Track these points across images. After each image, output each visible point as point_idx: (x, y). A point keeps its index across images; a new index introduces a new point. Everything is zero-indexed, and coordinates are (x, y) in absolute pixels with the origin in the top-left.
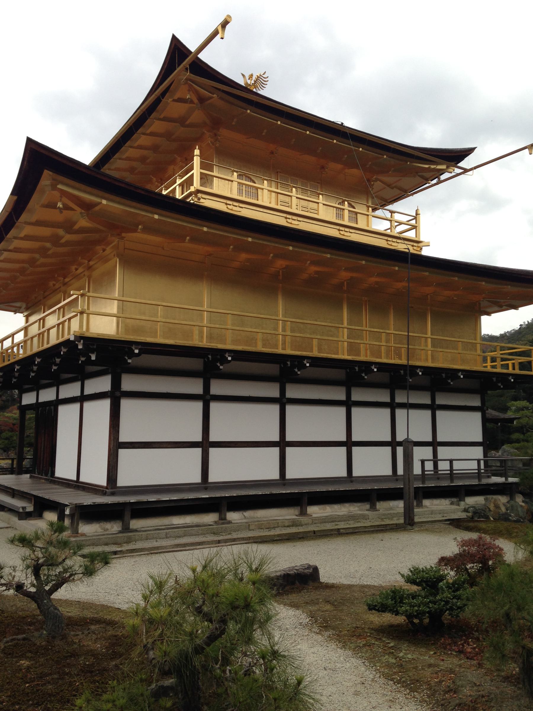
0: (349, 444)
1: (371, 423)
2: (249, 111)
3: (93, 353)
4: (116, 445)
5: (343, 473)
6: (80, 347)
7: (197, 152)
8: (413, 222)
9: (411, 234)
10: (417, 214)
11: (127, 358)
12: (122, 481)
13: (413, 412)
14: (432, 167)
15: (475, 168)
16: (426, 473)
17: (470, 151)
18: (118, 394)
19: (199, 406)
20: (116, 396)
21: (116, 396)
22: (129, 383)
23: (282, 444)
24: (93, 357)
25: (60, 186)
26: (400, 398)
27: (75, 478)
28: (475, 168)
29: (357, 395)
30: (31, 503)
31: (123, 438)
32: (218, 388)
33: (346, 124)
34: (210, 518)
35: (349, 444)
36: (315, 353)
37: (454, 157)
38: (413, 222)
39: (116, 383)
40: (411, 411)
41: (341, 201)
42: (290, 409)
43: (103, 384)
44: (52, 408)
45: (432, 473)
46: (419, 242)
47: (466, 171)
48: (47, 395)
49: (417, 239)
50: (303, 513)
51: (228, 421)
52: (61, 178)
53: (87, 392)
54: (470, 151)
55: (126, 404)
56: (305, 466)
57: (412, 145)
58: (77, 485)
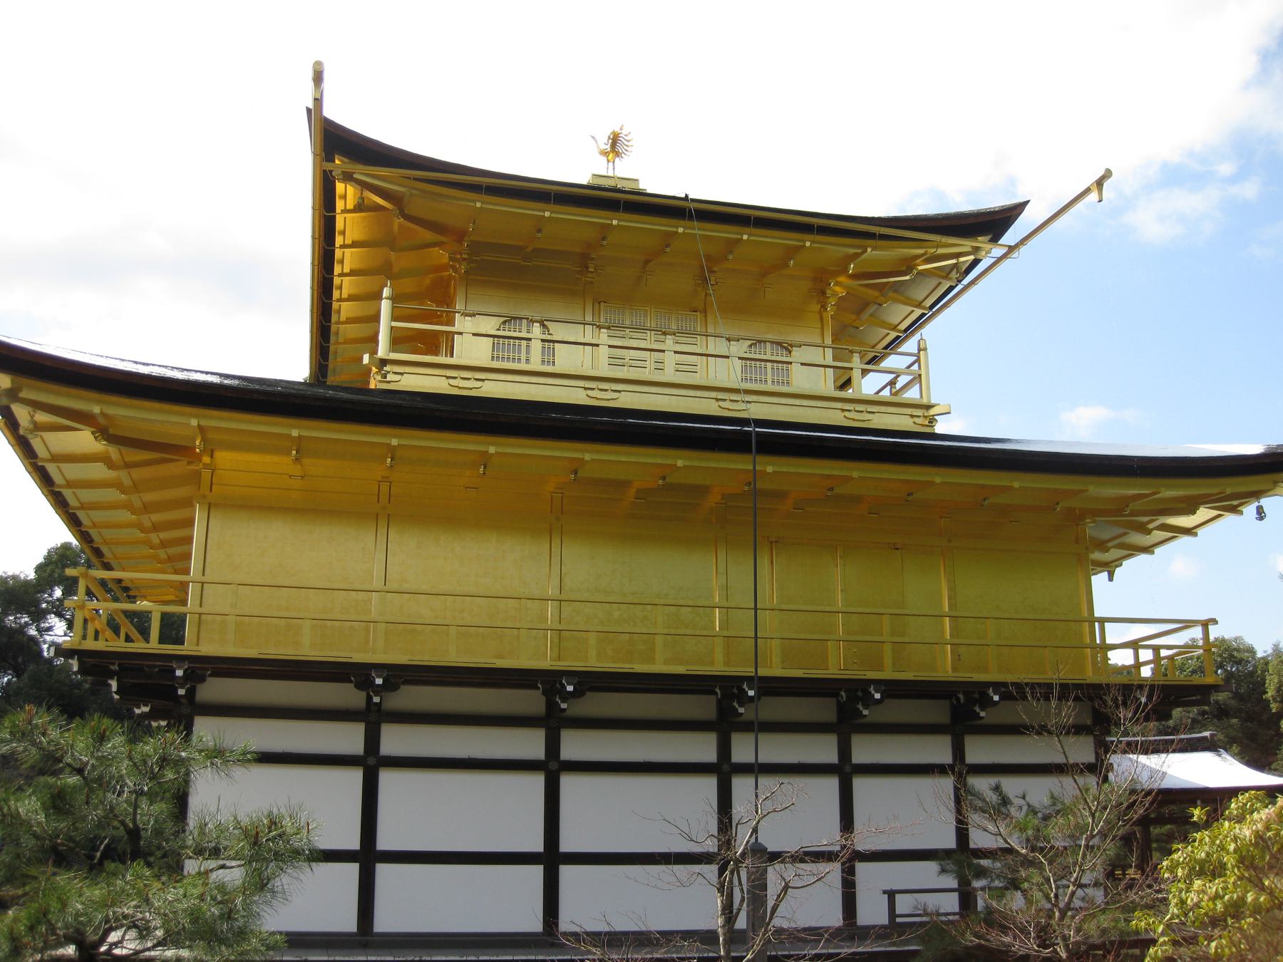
2: (478, 205)
3: (112, 678)
9: (913, 394)
10: (919, 350)
16: (898, 920)
25: (23, 395)
26: (742, 750)
37: (992, 224)
41: (750, 342)
42: (568, 783)
45: (957, 917)
46: (929, 407)
47: (1011, 249)
49: (925, 401)
51: (416, 809)
52: (25, 381)
57: (876, 216)
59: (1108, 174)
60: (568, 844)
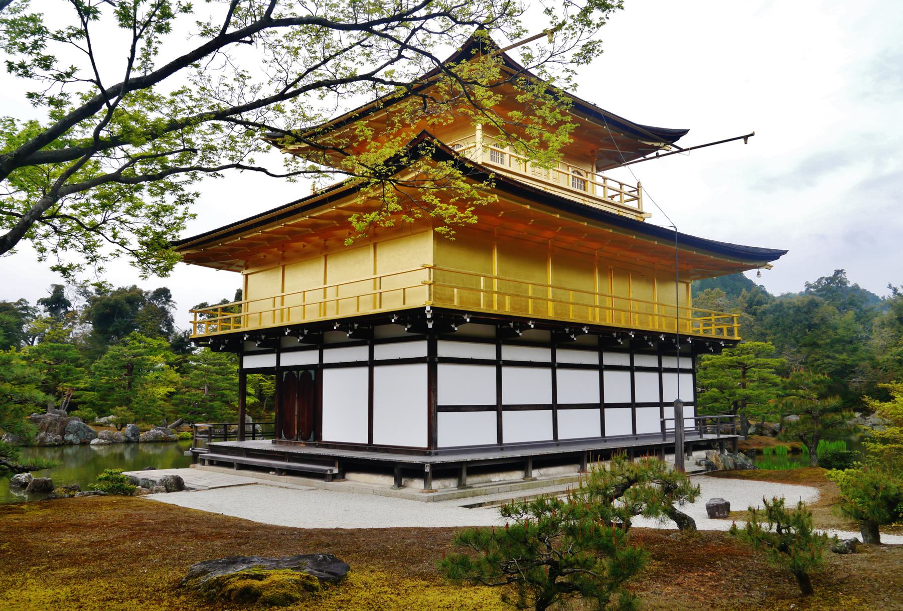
0: (602, 406)
1: (617, 386)
4: (434, 409)
5: (598, 434)
6: (429, 316)
8: (635, 193)
9: (634, 205)
11: (453, 326)
12: (441, 443)
13: (682, 376)
14: (656, 144)
15: (691, 149)
17: (684, 132)
18: (437, 360)
19: (493, 370)
20: (432, 361)
21: (432, 361)
22: (445, 349)
23: (554, 407)
24: (430, 326)
27: (365, 441)
28: (691, 149)
29: (610, 359)
30: (334, 466)
32: (510, 353)
33: (599, 105)
34: (517, 475)
35: (602, 406)
36: (590, 320)
37: (670, 137)
38: (635, 193)
39: (432, 349)
40: (681, 375)
43: (420, 349)
44: (312, 372)
46: (641, 213)
47: (681, 150)
48: (309, 358)
50: (583, 470)
53: (377, 357)
54: (685, 132)
55: (442, 369)
56: (579, 427)
58: (370, 446)
59: (752, 135)
60: (549, 401)
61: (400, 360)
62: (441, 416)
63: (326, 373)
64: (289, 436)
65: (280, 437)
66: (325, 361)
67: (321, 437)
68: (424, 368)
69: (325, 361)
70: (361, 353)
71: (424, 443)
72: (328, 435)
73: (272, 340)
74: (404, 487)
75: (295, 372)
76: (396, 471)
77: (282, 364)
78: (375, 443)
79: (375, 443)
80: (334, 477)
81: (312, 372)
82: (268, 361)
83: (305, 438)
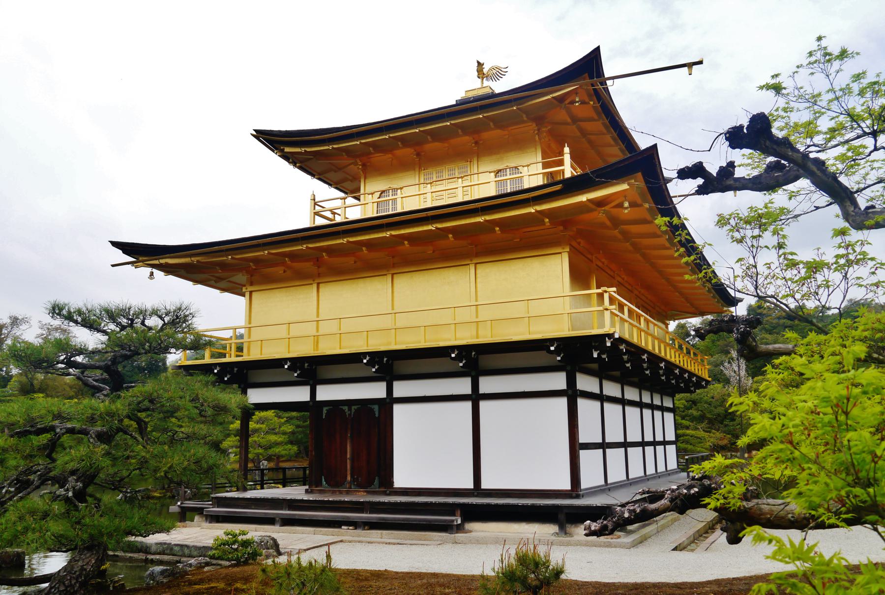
4: (575, 447)
7: (567, 150)
21: (572, 395)
30: (454, 515)
31: (583, 439)
44: (376, 408)
48: (376, 391)
61: (524, 393)
62: (583, 454)
63: (397, 409)
64: (336, 483)
65: (319, 484)
66: (397, 394)
67: (392, 483)
68: (563, 402)
69: (397, 394)
70: (463, 386)
71: (566, 485)
72: (400, 480)
73: (310, 369)
74: (571, 535)
75: (346, 408)
76: (562, 517)
77: (318, 399)
78: (483, 486)
79: (485, 485)
80: (459, 528)
81: (376, 408)
82: (300, 394)
83: (365, 485)
